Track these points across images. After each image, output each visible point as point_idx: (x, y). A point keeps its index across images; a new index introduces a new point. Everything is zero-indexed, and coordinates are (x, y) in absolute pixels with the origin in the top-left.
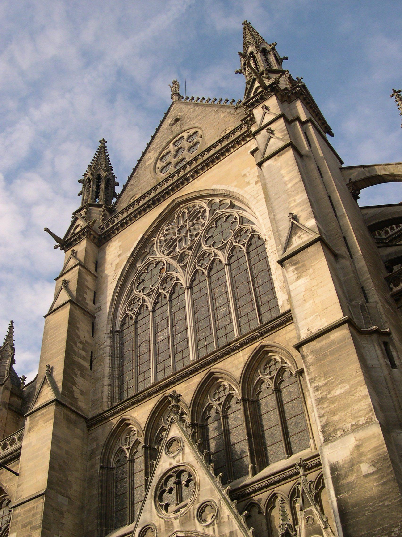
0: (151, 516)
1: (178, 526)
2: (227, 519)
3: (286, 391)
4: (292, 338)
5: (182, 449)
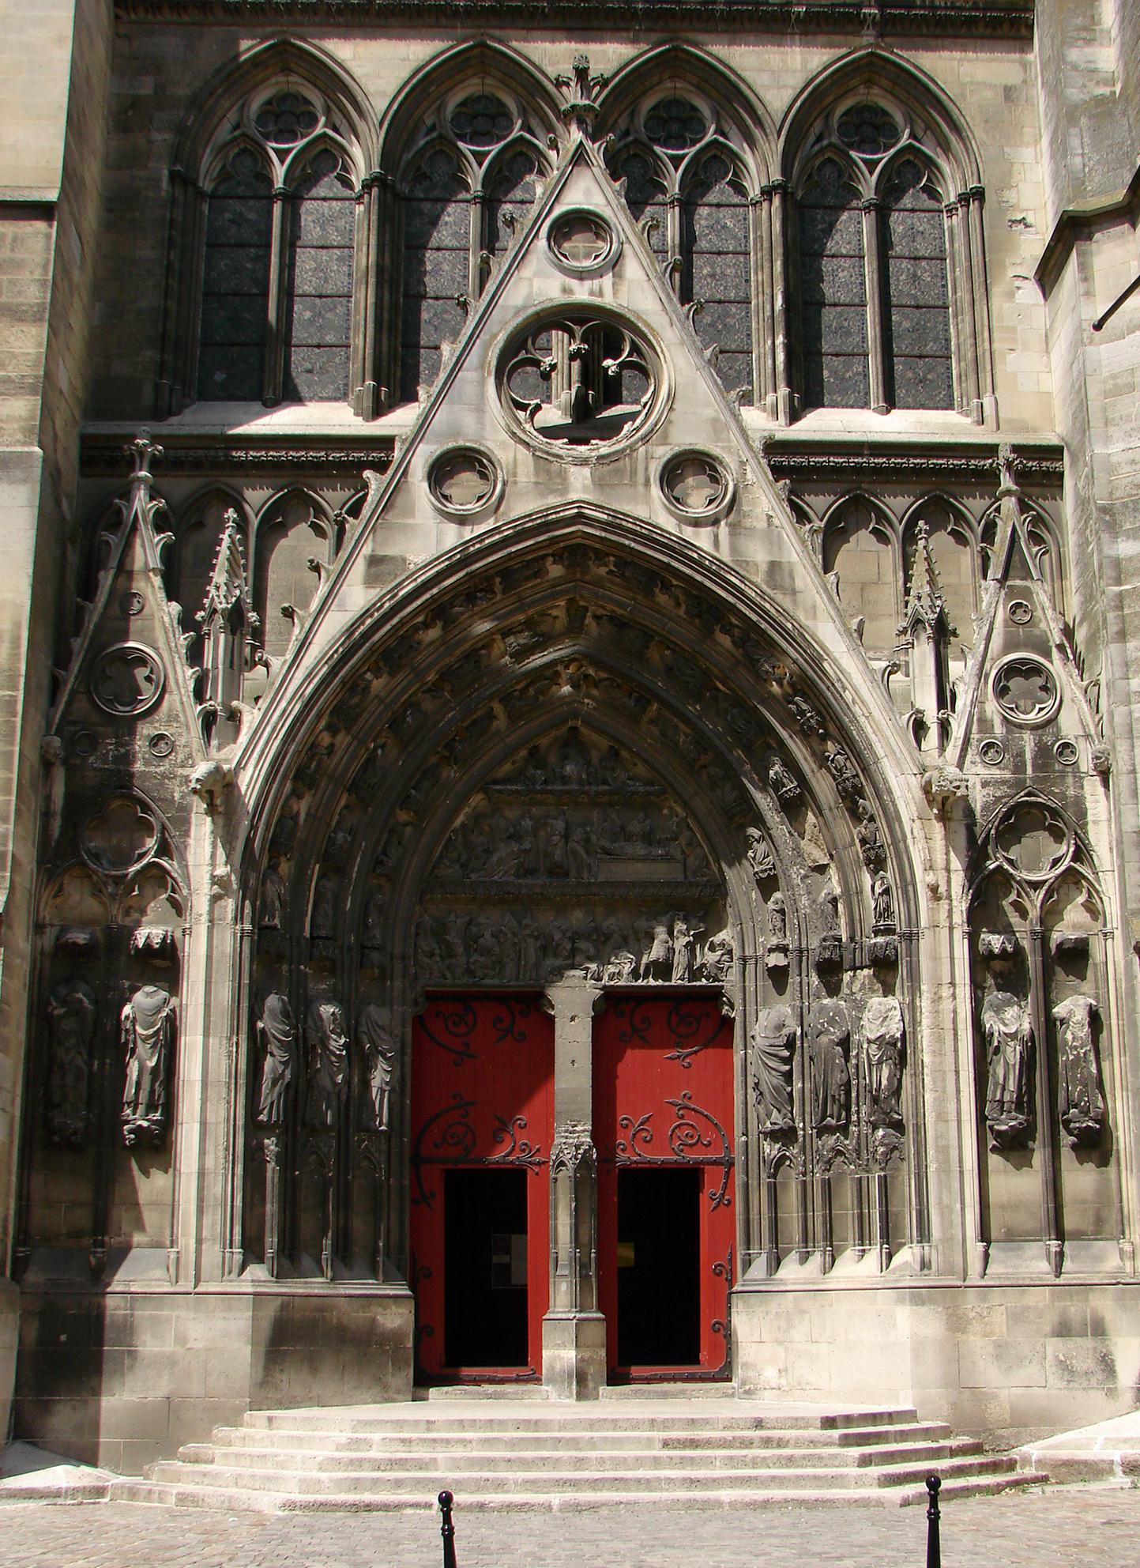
0: (481, 423)
1: (584, 486)
2: (766, 525)
3: (903, 222)
4: (978, 83)
5: (615, 263)
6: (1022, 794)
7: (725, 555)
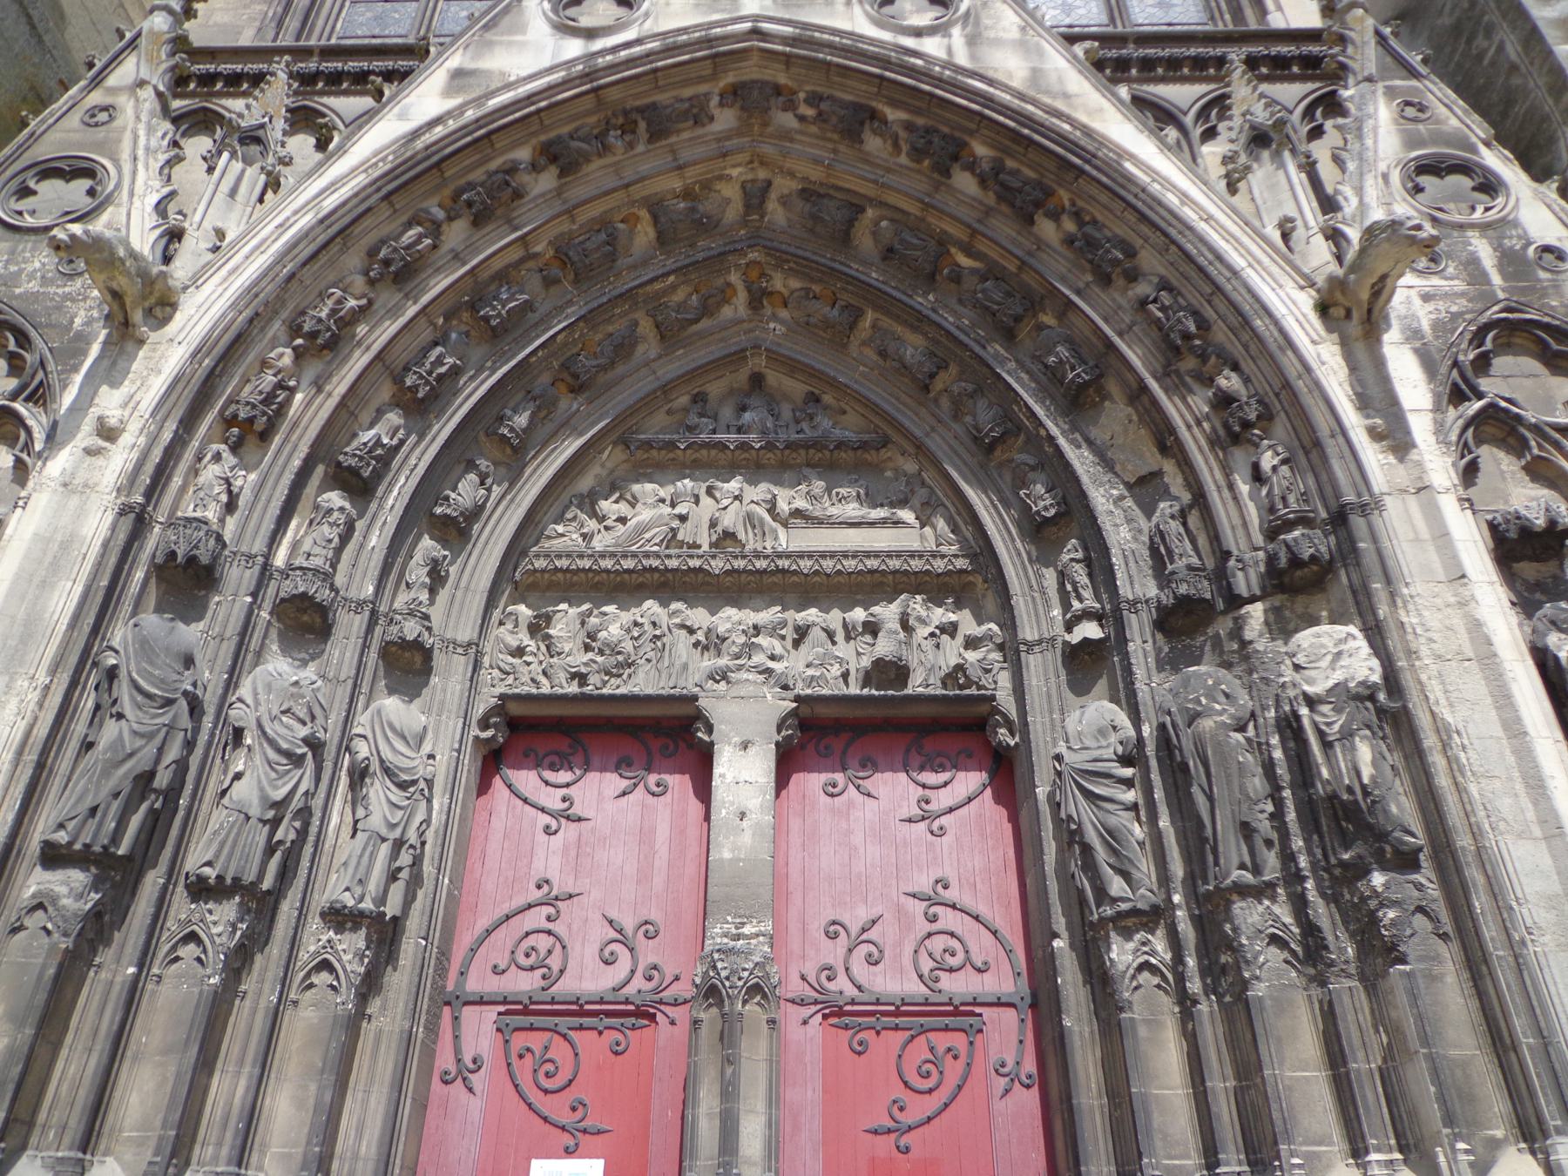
6: (1496, 308)
7: (962, 59)
